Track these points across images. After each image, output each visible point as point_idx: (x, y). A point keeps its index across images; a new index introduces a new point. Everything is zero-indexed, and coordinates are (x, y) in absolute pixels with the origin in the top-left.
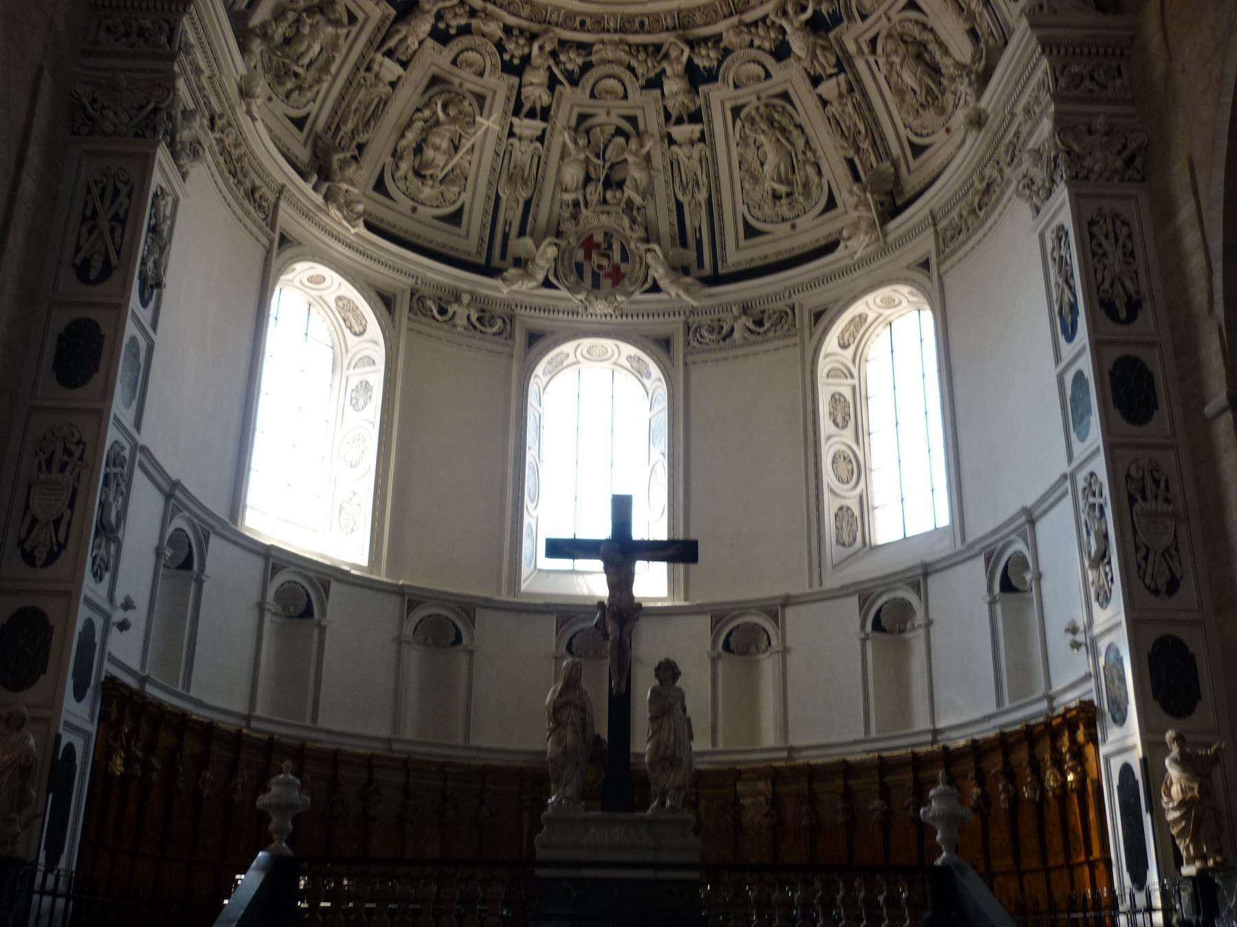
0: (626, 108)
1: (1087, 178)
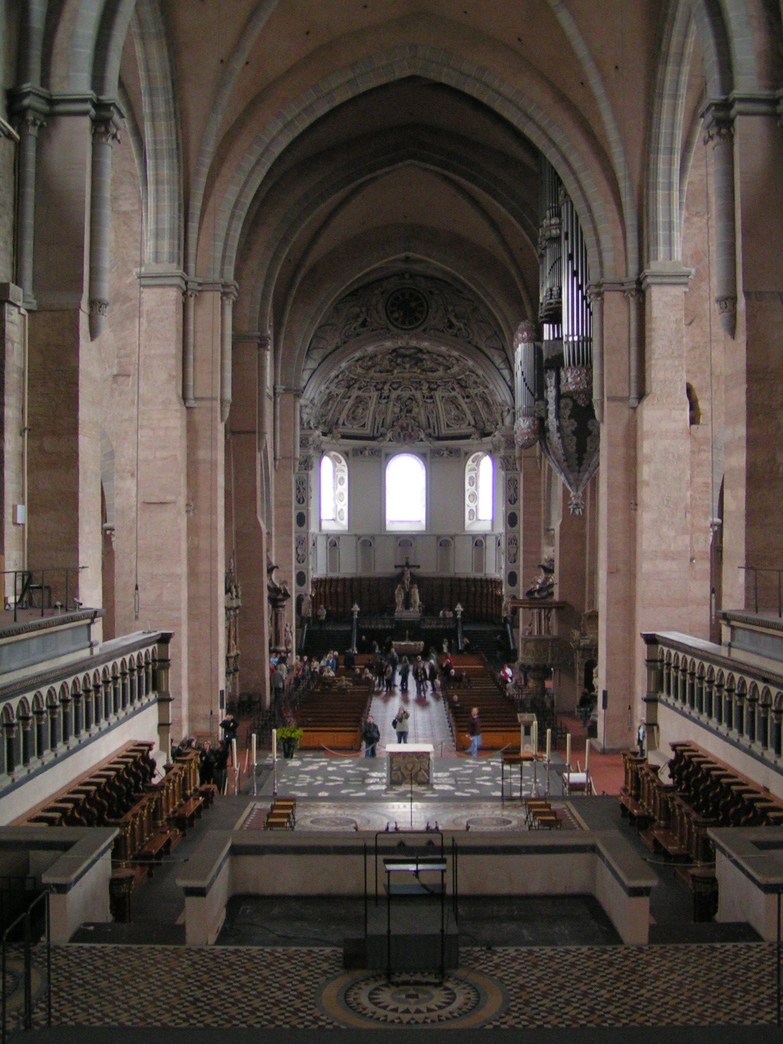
0: (411, 393)
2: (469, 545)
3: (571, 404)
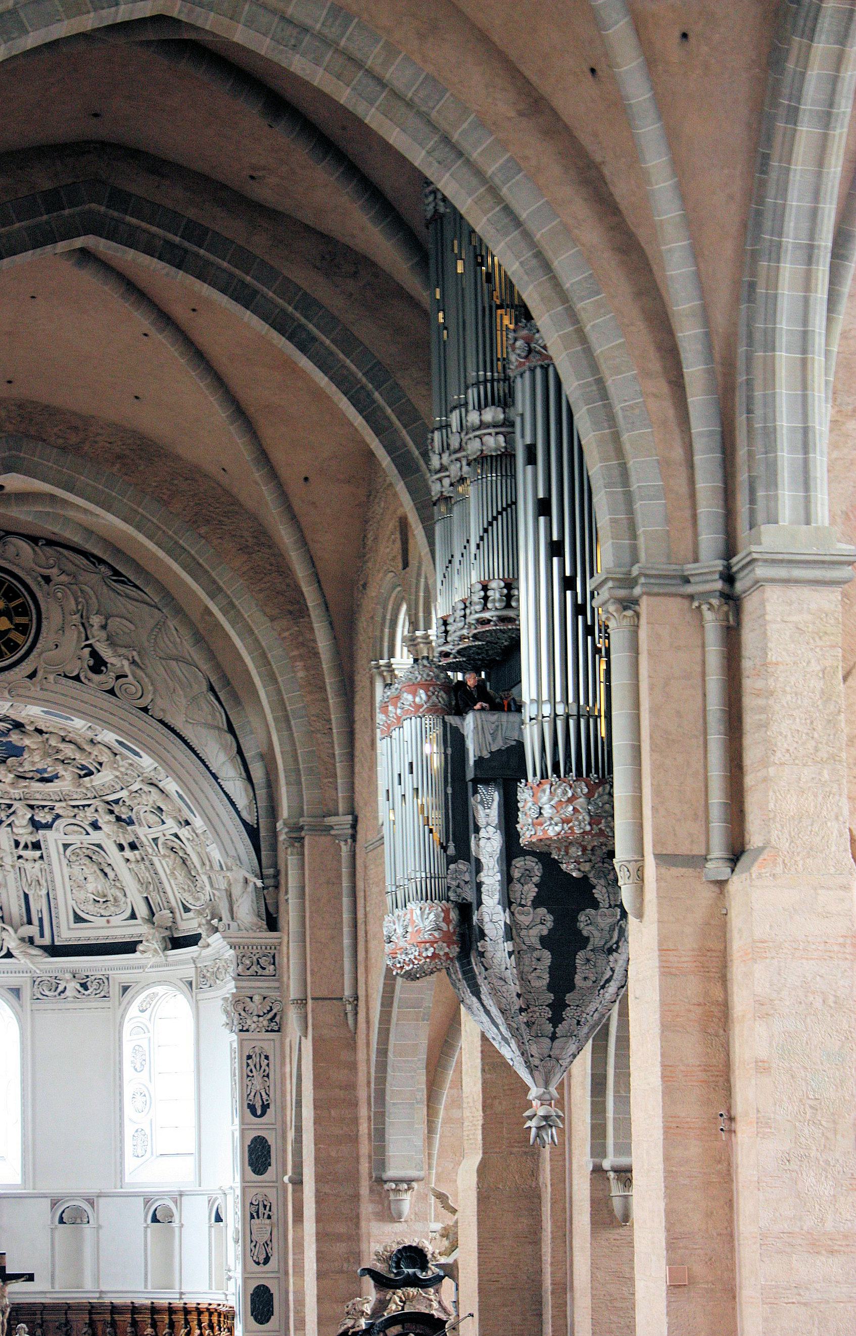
1: (247, 1030)
2: (138, 1215)
3: (537, 870)
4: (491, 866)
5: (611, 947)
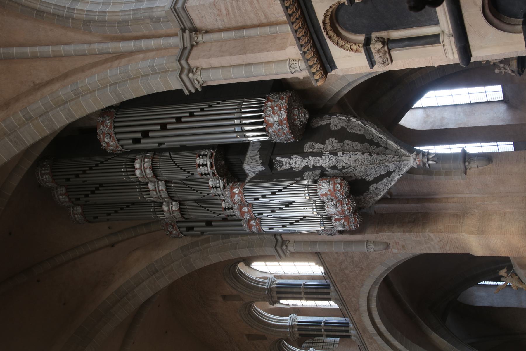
4: (306, 161)
5: (348, 120)
